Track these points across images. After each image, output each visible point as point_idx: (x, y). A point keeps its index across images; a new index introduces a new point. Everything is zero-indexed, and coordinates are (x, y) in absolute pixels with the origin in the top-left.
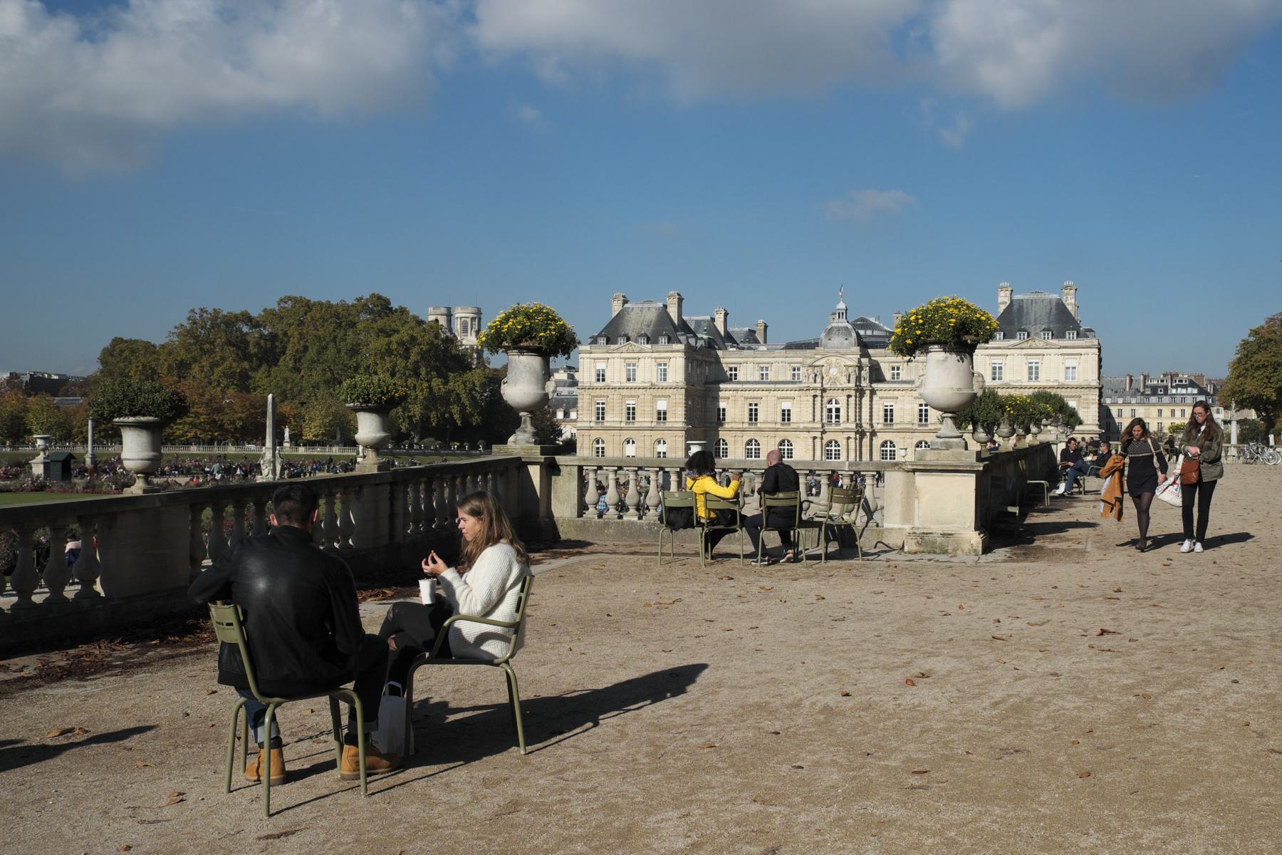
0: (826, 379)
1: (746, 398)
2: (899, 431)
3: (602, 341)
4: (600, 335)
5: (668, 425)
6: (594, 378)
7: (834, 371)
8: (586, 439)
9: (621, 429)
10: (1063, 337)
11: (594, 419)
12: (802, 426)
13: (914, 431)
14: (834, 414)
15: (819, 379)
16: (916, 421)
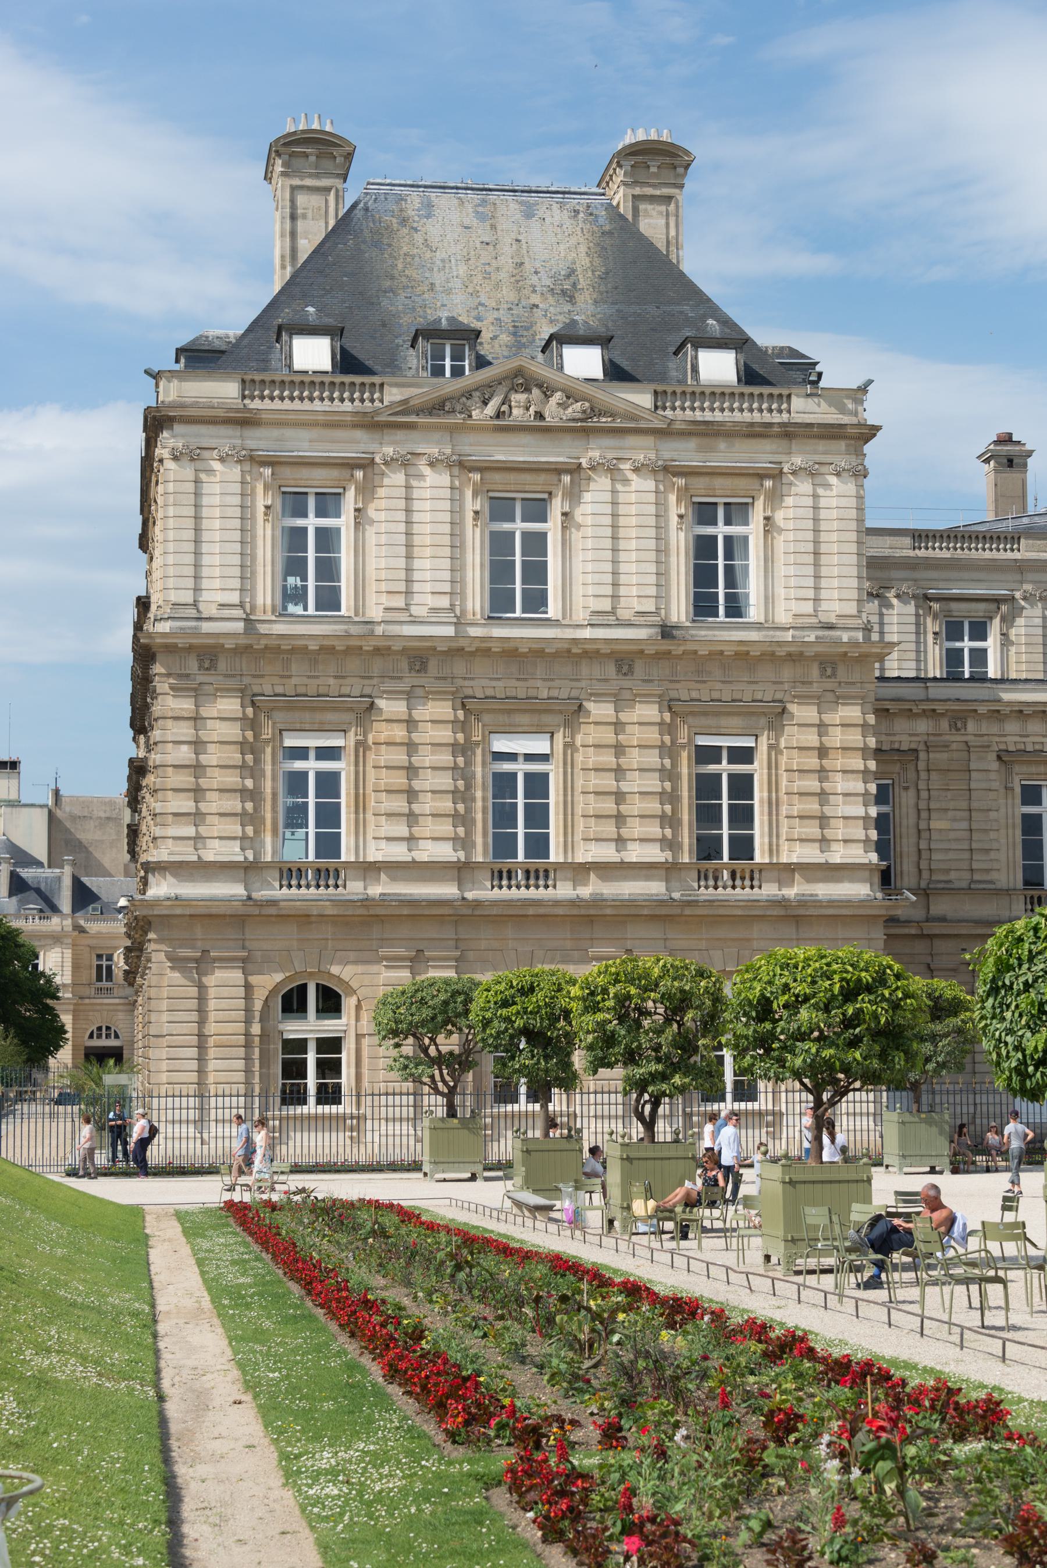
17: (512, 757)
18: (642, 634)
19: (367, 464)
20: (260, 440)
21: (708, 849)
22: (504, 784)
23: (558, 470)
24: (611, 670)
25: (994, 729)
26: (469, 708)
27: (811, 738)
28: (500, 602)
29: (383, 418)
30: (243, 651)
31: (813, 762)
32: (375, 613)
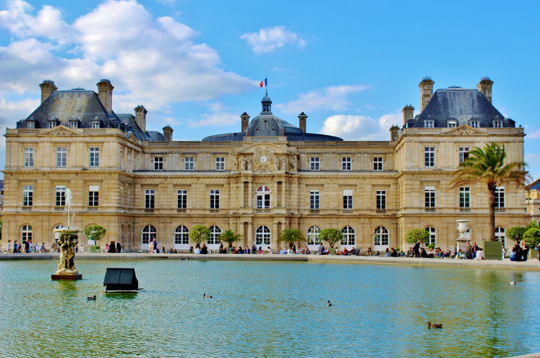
0: (256, 166)
1: (175, 186)
2: (325, 217)
3: (31, 125)
4: (28, 120)
5: (99, 210)
6: (22, 163)
7: (264, 159)
8: (13, 224)
9: (50, 214)
10: (491, 126)
11: (21, 204)
12: (231, 212)
13: (338, 217)
14: (263, 200)
15: (249, 167)
16: (342, 207)
17: (59, 189)
18: (79, 169)
19: (37, 143)
20: (21, 139)
21: (91, 204)
22: (58, 194)
23: (66, 143)
24: (75, 175)
25: (172, 180)
26: (52, 181)
27: (107, 186)
28: (59, 164)
29: (39, 135)
30: (16, 173)
31: (107, 190)
32: (38, 166)
